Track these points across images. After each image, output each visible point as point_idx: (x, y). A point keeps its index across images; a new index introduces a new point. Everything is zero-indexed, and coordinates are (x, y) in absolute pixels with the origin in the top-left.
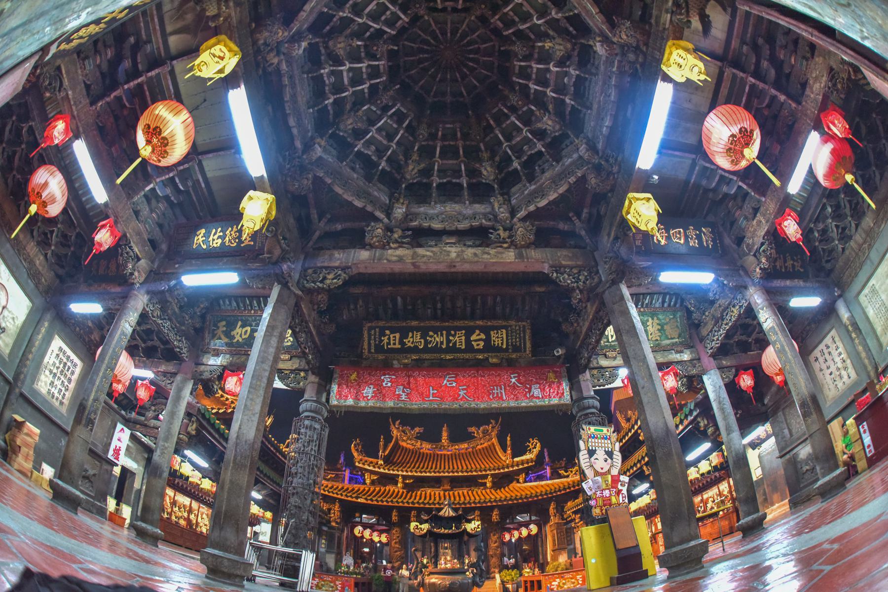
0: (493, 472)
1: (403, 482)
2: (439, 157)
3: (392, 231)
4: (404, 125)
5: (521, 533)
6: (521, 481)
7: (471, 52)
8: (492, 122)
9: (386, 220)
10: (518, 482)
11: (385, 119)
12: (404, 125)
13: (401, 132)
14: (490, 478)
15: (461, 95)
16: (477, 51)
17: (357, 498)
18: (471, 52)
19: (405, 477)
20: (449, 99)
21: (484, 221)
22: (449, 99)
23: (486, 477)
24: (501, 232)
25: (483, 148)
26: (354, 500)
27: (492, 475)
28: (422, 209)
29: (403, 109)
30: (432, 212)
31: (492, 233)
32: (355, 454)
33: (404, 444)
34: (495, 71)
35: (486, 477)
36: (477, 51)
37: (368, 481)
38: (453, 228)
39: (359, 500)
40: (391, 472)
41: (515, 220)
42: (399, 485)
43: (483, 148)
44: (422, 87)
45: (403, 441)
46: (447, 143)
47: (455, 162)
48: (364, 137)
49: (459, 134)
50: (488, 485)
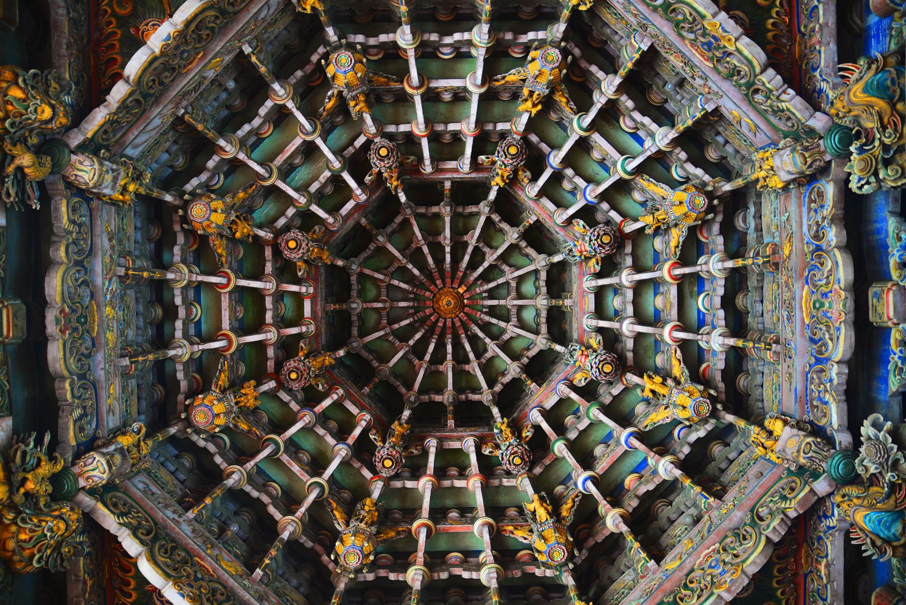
2: (239, 289)
3: (38, 151)
4: (314, 208)
7: (457, 345)
8: (327, 403)
9: (75, 140)
11: (337, 165)
12: (314, 208)
13: (303, 200)
15: (363, 334)
16: (460, 358)
18: (457, 345)
20: (357, 306)
21: (77, 413)
22: (357, 306)
24: (46, 469)
25: (265, 387)
28: (103, 243)
29: (350, 205)
30: (99, 268)
31: (39, 442)
34: (425, 398)
36: (460, 358)
38: (51, 328)
41: (87, 500)
43: (265, 387)
44: (382, 250)
46: (269, 302)
47: (226, 324)
48: (298, 109)
49: (293, 331)
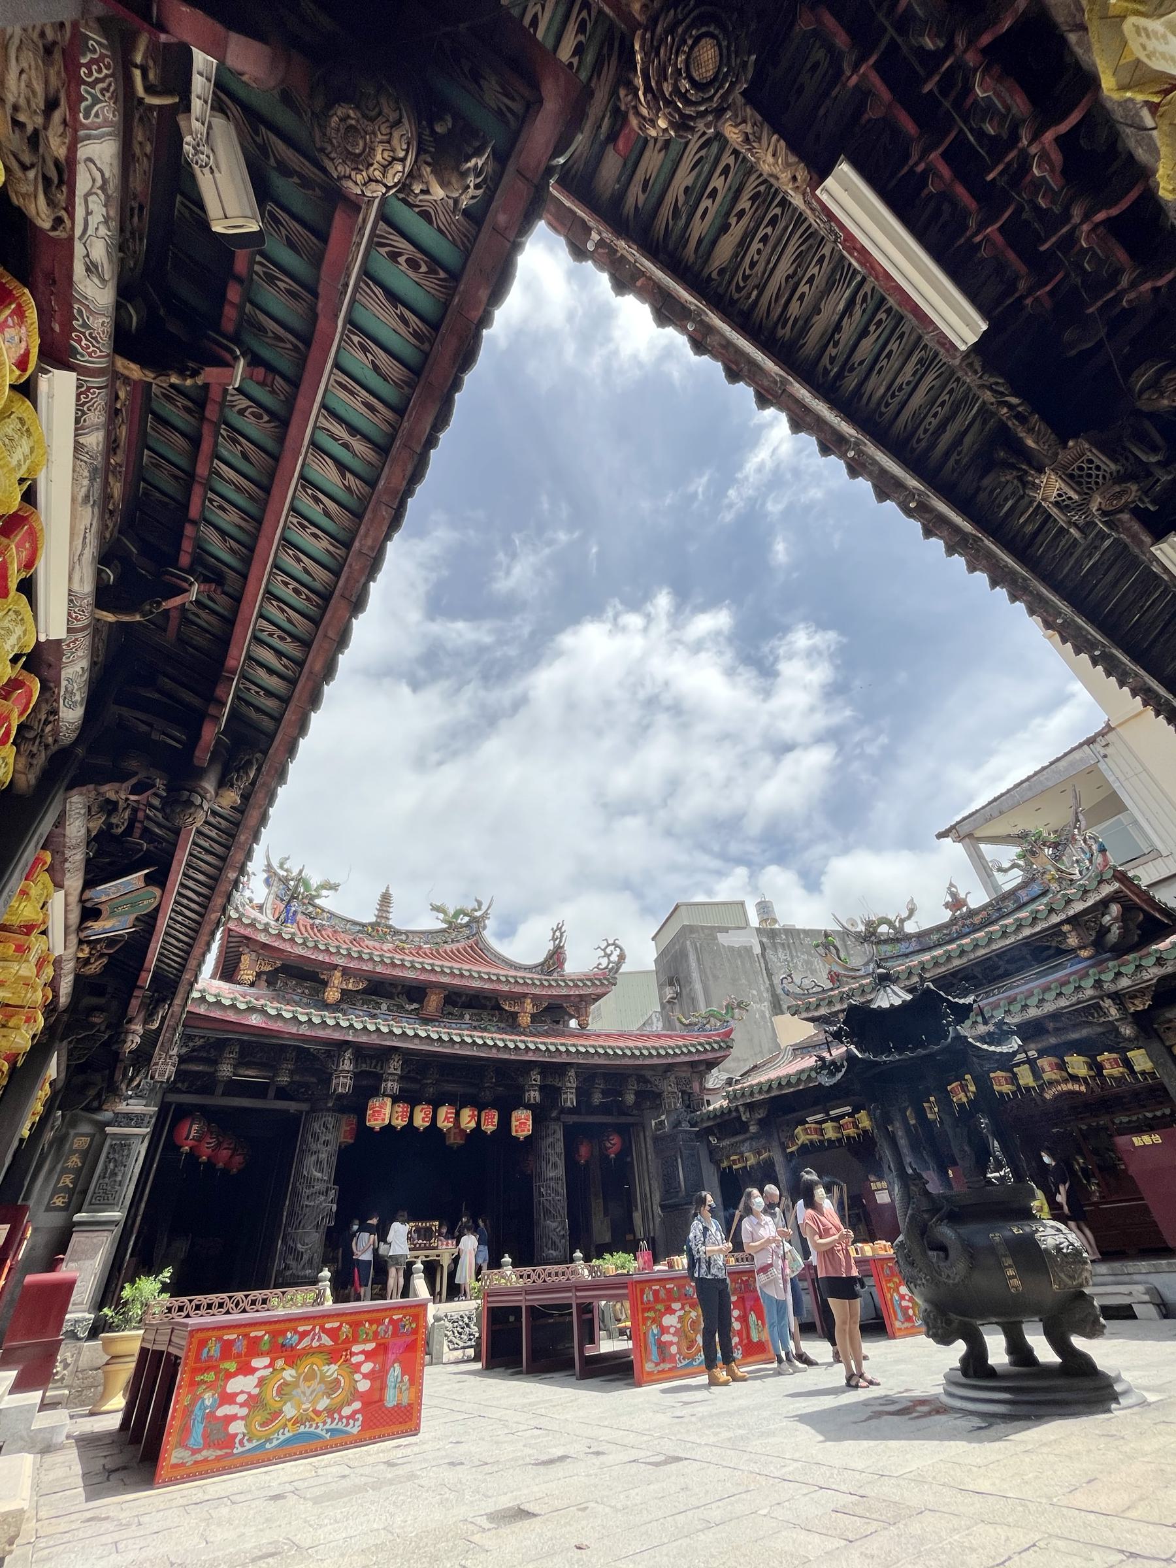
42: (332, 995)
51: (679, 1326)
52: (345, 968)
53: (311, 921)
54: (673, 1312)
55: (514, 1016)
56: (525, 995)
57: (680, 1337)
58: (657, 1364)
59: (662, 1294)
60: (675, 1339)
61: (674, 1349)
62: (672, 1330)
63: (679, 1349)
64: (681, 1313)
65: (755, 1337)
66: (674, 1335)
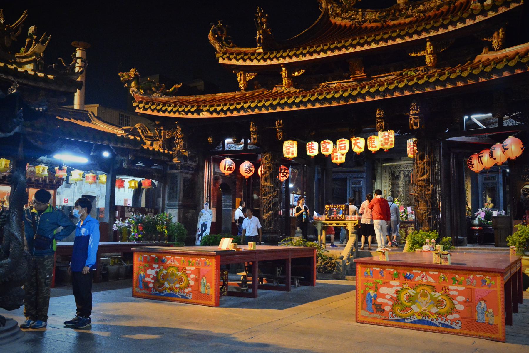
0: (432, 34)
1: (289, 76)
5: (491, 156)
6: (495, 43)
10: (492, 49)
14: (429, 48)
17: (198, 112)
19: (291, 67)
23: (420, 45)
26: (195, 116)
27: (432, 39)
32: (217, 46)
33: (338, 21)
35: (420, 45)
37: (241, 85)
39: (201, 116)
40: (269, 62)
42: (285, 81)
45: (337, 15)
50: (429, 60)
51: (155, 275)
52: (286, 65)
53: (351, 22)
54: (153, 268)
55: (424, 57)
56: (424, 40)
57: (155, 280)
58: (141, 290)
59: (149, 259)
60: (153, 281)
61: (151, 285)
62: (152, 277)
63: (154, 285)
64: (158, 270)
65: (203, 290)
66: (152, 279)
